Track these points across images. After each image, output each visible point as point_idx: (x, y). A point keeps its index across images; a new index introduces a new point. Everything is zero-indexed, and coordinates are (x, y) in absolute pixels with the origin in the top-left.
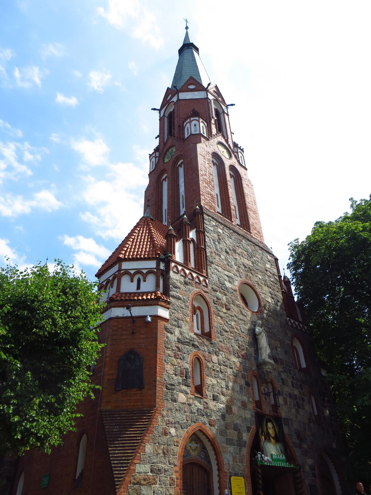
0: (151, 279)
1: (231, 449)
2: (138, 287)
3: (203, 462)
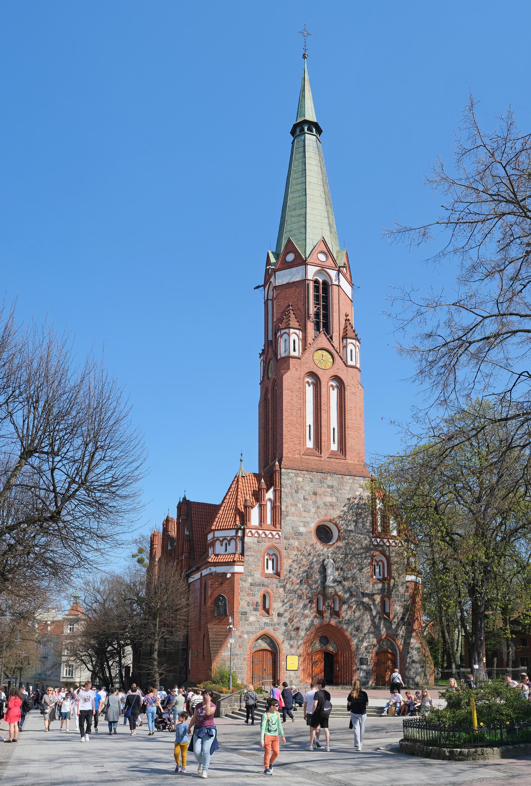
0: (233, 542)
2: (226, 550)
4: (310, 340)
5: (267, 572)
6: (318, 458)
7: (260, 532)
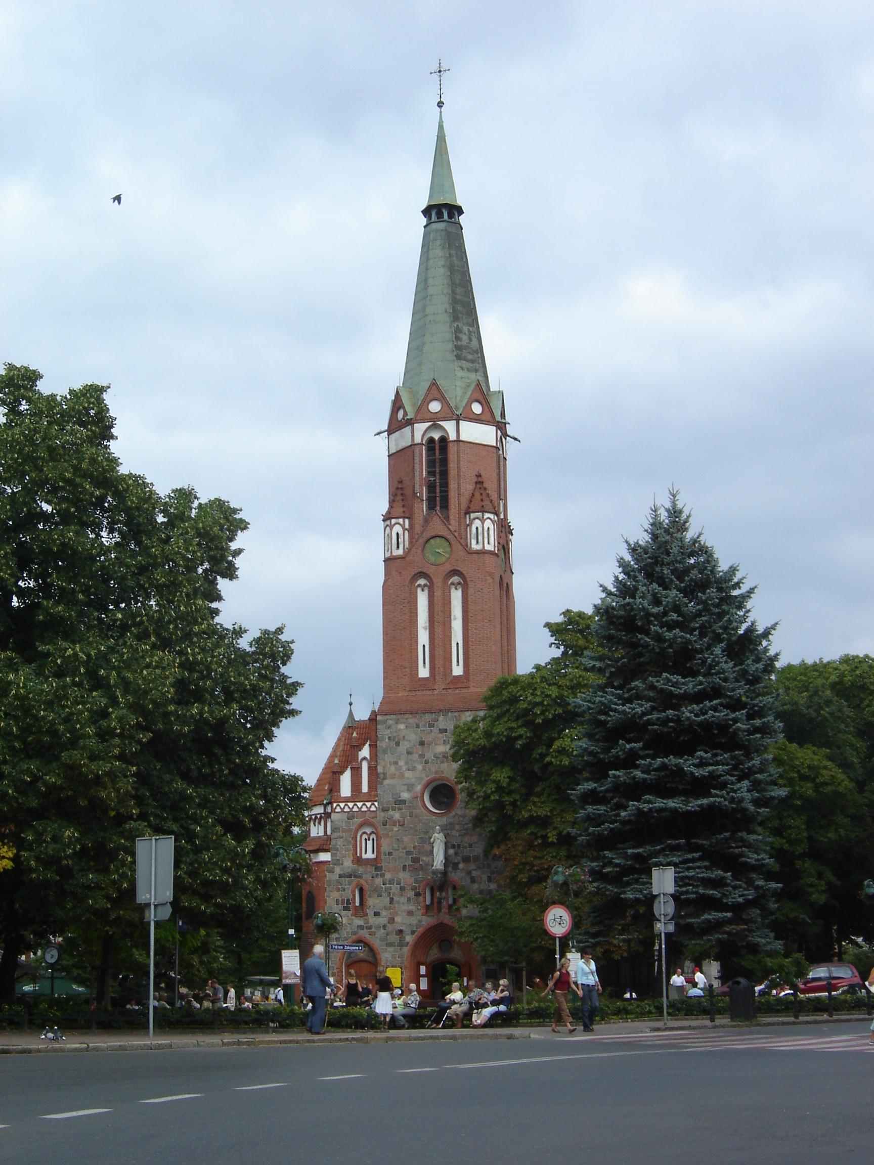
1: (391, 949)
3: (371, 959)
4: (418, 528)
5: (364, 856)
6: (430, 693)
7: (351, 805)
